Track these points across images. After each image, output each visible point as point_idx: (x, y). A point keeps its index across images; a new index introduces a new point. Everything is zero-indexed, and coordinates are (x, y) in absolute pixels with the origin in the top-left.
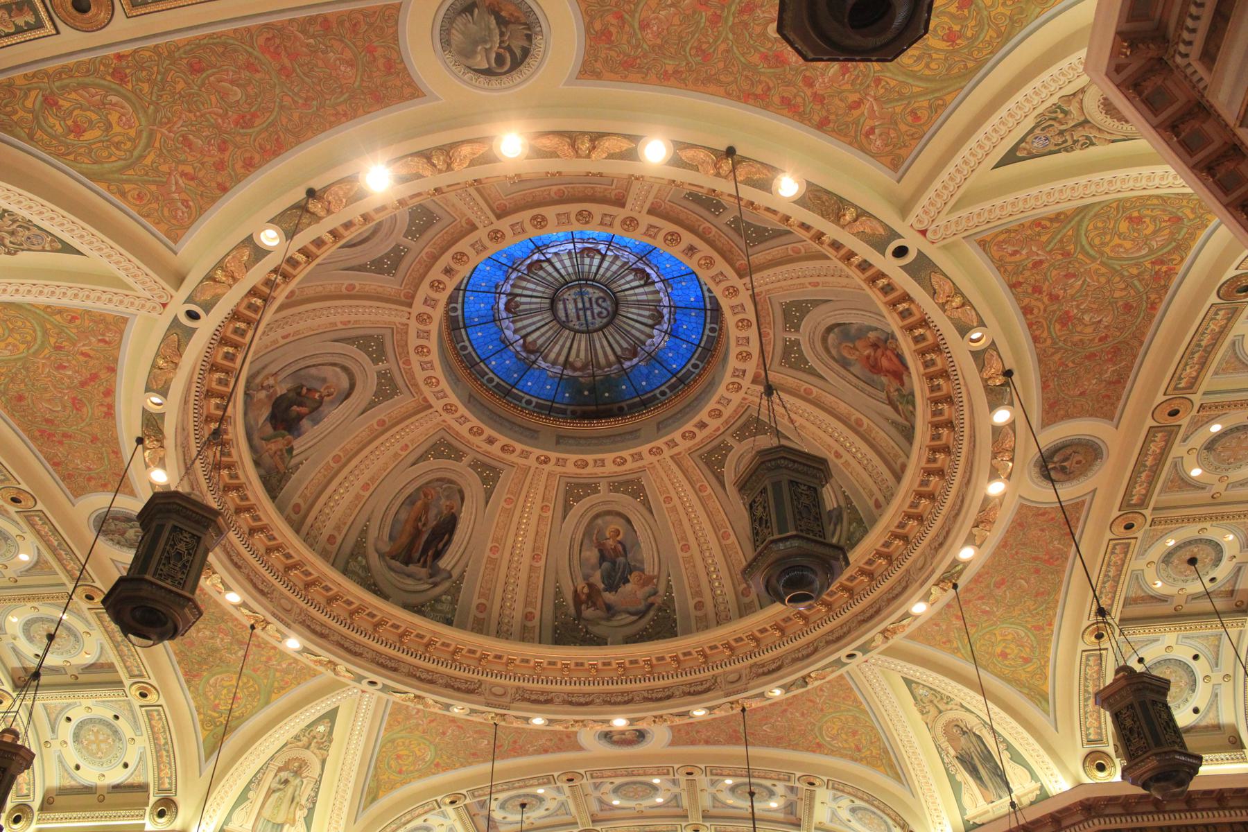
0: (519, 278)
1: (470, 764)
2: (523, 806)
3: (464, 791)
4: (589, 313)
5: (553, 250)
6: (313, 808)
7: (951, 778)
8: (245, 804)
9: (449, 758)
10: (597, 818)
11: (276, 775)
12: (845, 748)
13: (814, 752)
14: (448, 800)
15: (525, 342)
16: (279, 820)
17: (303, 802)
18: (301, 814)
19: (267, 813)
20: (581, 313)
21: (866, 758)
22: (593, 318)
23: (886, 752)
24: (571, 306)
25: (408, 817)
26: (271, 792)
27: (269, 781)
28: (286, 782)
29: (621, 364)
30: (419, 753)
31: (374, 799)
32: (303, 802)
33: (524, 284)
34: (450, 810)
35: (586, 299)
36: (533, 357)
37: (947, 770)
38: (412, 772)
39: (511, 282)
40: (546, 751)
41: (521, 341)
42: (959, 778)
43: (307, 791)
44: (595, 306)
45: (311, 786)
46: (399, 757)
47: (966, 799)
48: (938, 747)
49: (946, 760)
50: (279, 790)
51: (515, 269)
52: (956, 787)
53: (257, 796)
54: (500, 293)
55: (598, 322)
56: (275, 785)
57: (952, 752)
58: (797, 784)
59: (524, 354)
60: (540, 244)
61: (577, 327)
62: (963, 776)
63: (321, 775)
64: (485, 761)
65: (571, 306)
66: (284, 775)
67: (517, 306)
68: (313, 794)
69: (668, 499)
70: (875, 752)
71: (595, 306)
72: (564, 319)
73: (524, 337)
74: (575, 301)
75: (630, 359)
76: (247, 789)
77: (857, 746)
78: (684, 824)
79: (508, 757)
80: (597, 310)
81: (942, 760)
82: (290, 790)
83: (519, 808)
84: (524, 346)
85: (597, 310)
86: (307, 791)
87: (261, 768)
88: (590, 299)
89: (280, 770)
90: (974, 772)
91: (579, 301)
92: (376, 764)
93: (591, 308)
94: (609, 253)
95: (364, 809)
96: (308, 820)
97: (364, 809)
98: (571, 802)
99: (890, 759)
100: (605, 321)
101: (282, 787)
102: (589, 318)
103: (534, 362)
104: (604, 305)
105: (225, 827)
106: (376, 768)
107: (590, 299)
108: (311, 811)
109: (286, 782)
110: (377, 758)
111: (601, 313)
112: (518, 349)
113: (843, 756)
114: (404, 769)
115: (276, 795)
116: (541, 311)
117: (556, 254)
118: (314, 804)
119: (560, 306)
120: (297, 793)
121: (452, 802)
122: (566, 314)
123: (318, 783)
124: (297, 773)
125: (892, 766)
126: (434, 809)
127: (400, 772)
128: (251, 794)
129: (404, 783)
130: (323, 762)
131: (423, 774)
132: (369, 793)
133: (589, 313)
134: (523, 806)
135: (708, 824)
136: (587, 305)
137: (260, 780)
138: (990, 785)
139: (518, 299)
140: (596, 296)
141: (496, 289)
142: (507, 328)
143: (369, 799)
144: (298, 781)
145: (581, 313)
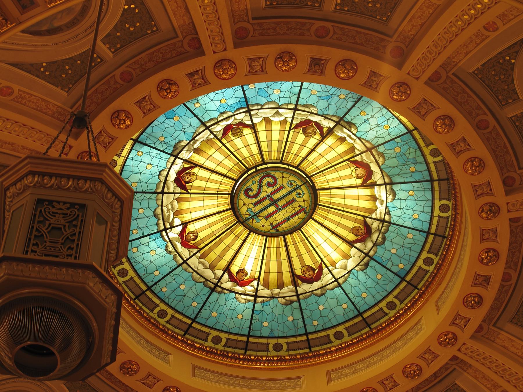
0: (266, 285)
4: (276, 196)
5: (209, 274)
15: (357, 241)
20: (281, 203)
22: (282, 187)
24: (279, 217)
29: (330, 131)
33: (273, 276)
35: (259, 208)
36: (375, 225)
39: (276, 291)
41: (358, 245)
44: (263, 195)
51: (256, 296)
54: (298, 295)
55: (283, 180)
59: (375, 236)
60: (207, 291)
61: (306, 197)
65: (279, 217)
67: (310, 268)
69: (490, 27)
71: (263, 195)
72: (302, 215)
73: (351, 244)
74: (267, 217)
75: (318, 125)
80: (266, 190)
84: (362, 240)
85: (266, 190)
88: (256, 204)
91: (265, 213)
93: (269, 196)
94: (177, 222)
100: (277, 175)
102: (284, 192)
103: (382, 221)
104: (255, 187)
107: (256, 204)
111: (269, 185)
112: (370, 245)
116: (329, 208)
117: (212, 267)
119: (285, 226)
122: (292, 216)
133: (276, 196)
136: (267, 202)
139: (298, 272)
140: (247, 200)
141: (292, 302)
142: (345, 268)
145: (281, 203)
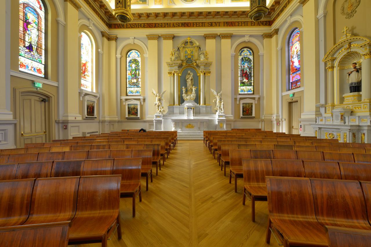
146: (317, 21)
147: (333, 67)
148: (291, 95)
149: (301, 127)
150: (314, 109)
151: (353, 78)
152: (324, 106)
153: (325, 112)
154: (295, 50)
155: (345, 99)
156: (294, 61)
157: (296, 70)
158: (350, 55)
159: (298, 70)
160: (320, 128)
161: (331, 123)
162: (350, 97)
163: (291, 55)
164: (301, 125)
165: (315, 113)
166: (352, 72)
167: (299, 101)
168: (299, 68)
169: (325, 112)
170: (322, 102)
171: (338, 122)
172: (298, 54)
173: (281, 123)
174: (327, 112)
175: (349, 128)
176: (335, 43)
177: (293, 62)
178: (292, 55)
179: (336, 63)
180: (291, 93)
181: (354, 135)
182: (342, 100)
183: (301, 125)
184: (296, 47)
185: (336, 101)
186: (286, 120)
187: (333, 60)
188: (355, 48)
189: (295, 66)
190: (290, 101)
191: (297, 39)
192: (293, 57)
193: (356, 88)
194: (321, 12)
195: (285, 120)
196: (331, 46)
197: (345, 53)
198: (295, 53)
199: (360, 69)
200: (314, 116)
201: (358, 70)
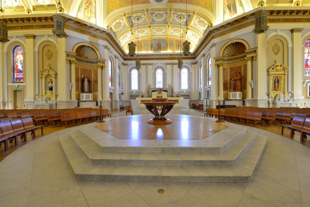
1: (127, 6)
2: (138, 19)
3: (126, 13)
6: (96, 14)
7: (224, 10)
8: (80, 12)
9: (122, 4)
10: (151, 23)
11: (85, 5)
12: (203, 4)
13: (196, 5)
14: (123, 15)
16: (89, 16)
17: (93, 12)
18: (93, 15)
19: (86, 14)
21: (207, 7)
23: (212, 5)
25: (116, 18)
26: (85, 9)
27: (84, 6)
28: (88, 7)
30: (116, 2)
31: (108, 13)
32: (93, 12)
34: (124, 18)
37: (224, 9)
38: (115, 7)
40: (142, 3)
42: (226, 11)
43: (93, 10)
45: (94, 8)
46: (112, 2)
47: (226, 16)
48: (224, 3)
49: (224, 7)
50: (87, 9)
52: (224, 12)
53: (82, 9)
56: (86, 7)
57: (227, 4)
58: (191, 14)
62: (227, 10)
63: (96, 6)
64: (130, 5)
66: (87, 5)
68: (95, 11)
70: (210, 5)
76: (79, 8)
77: (206, 3)
78: (167, 25)
79: (135, 4)
81: (224, 6)
82: (89, 9)
83: (137, 20)
86: (93, 10)
87: (81, 2)
89: (86, 3)
90: (230, 9)
92: (107, 4)
95: (107, 16)
96: (95, 16)
97: (107, 16)
98: (147, 19)
99: (212, 7)
101: (87, 8)
105: (77, 16)
106: (107, 5)
108: (95, 14)
109: (88, 7)
110: (107, 2)
113: (202, 6)
114: (114, 6)
115: (87, 10)
118: (96, 13)
120: (91, 10)
121: (124, 15)
123: (95, 7)
124: (90, 4)
125: (212, 9)
126: (121, 17)
127: (113, 7)
128: (81, 9)
129: (114, 10)
130: (95, 2)
131: (118, 8)
132: (107, 12)
134: (138, 19)
135: (171, 25)
137: (82, 5)
138: (232, 12)
143: (107, 13)
144: (90, 7)
146: (34, 52)
147: (42, 78)
148: (17, 86)
149: (24, 106)
150: (33, 96)
151: (50, 85)
152: (38, 95)
153: (39, 98)
154: (19, 59)
155: (47, 93)
156: (18, 65)
157: (20, 71)
158: (48, 75)
159: (20, 71)
160: (37, 106)
161: (42, 103)
162: (49, 92)
163: (16, 61)
164: (24, 105)
165: (33, 99)
166: (49, 82)
167: (23, 91)
168: (23, 71)
169: (39, 98)
170: (37, 93)
171: (44, 103)
172: (21, 62)
173: (7, 104)
174: (40, 98)
175: (49, 105)
176: (43, 68)
177: (17, 66)
178: (16, 61)
179: (43, 77)
180: (16, 85)
181: (50, 107)
182: (46, 93)
183: (24, 105)
184: (19, 57)
185: (44, 94)
186: (12, 102)
187: (42, 75)
188: (51, 73)
189: (19, 69)
190: (15, 90)
191: (21, 52)
192: (17, 62)
193: (51, 89)
194: (36, 49)
195: (11, 102)
196: (41, 69)
197: (47, 74)
198: (19, 61)
199: (52, 82)
200: (33, 100)
201: (52, 82)
